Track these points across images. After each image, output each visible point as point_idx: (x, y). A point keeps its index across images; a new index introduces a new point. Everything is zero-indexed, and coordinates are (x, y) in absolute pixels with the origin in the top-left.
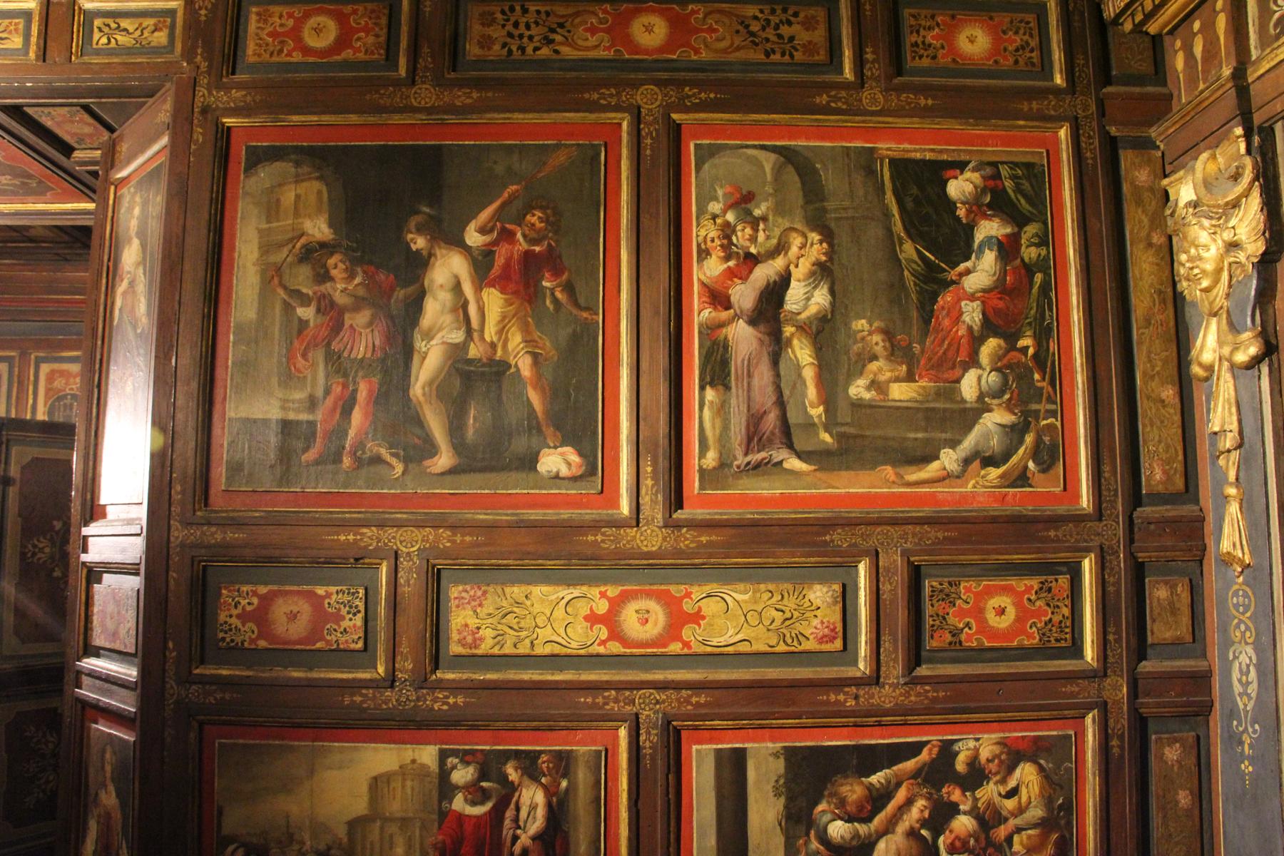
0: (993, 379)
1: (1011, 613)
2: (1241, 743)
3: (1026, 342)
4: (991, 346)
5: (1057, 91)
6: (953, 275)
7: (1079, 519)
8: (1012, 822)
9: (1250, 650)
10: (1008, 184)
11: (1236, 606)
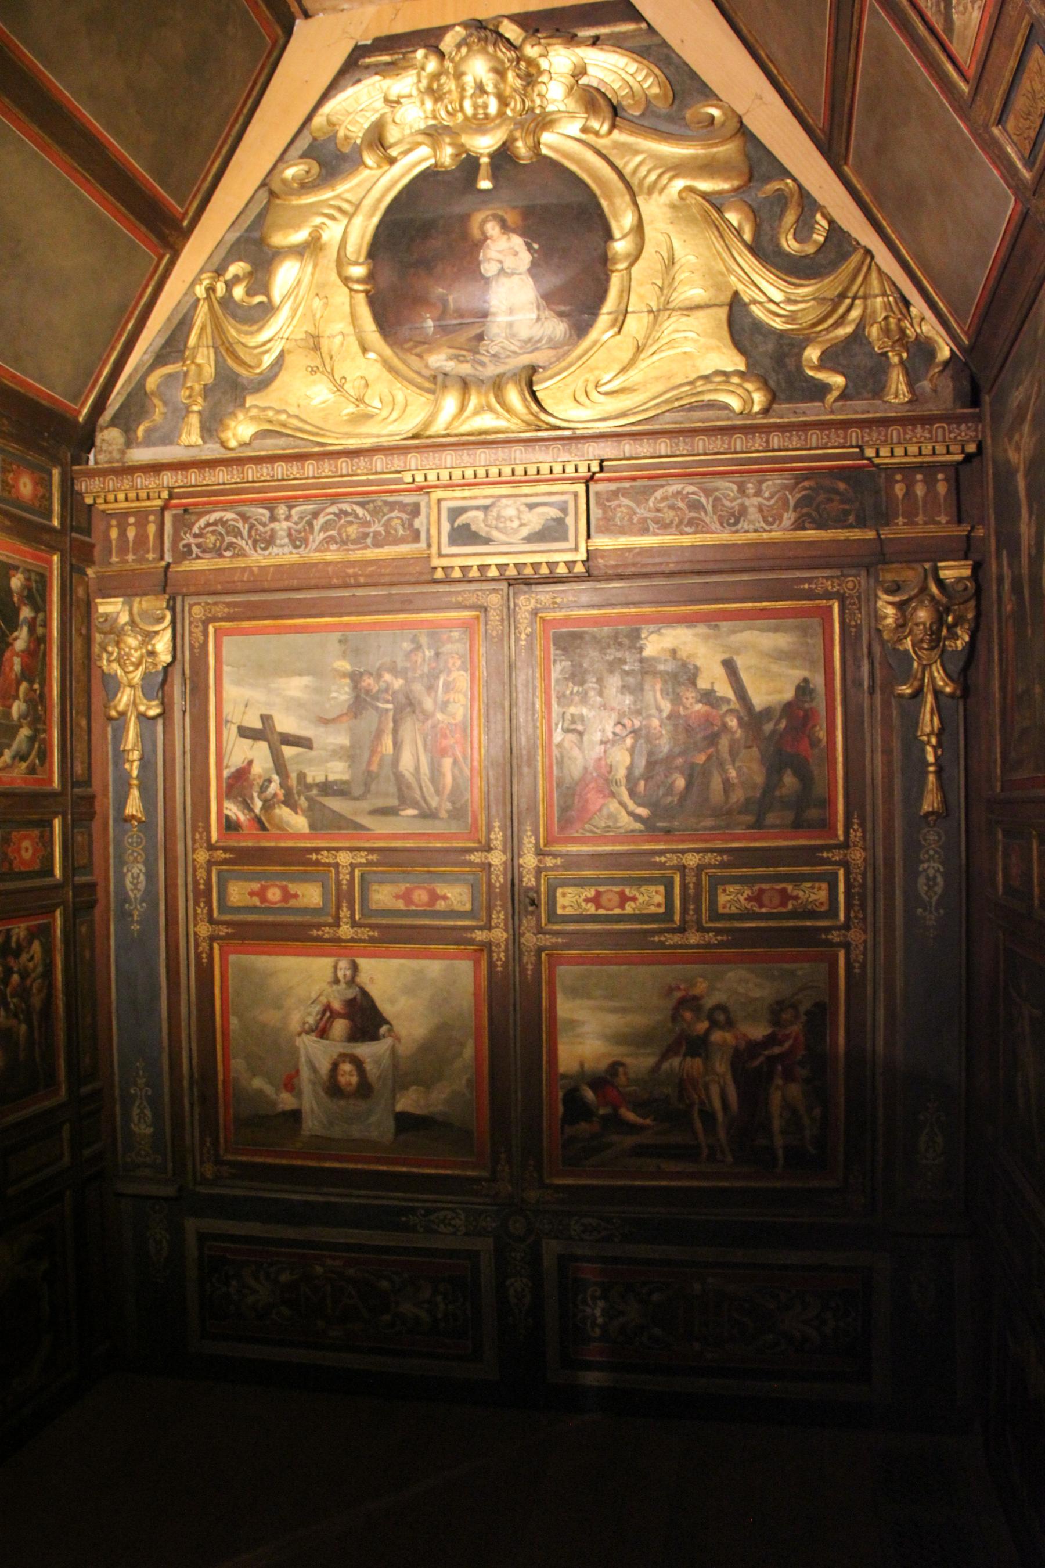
0: (23, 707)
1: (30, 851)
2: (132, 915)
3: (36, 686)
4: (24, 686)
5: (52, 530)
6: (10, 640)
7: (54, 794)
8: (33, 975)
9: (141, 866)
10: (34, 585)
11: (131, 844)
